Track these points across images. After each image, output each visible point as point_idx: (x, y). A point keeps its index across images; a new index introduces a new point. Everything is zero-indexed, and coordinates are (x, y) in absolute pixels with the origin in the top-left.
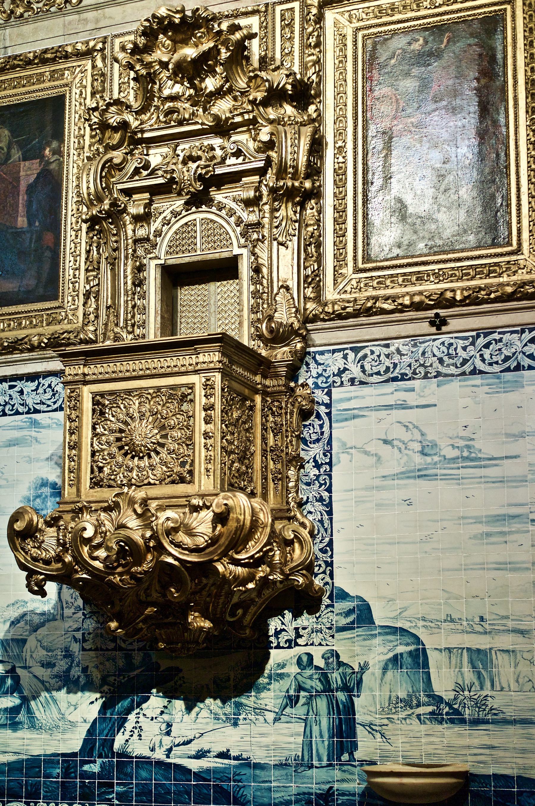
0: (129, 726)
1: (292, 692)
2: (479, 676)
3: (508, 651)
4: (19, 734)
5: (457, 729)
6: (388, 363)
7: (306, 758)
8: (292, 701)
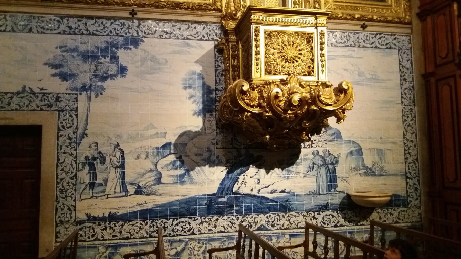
0: (240, 181)
1: (311, 166)
2: (381, 159)
3: (390, 150)
4: (185, 186)
5: (374, 178)
6: (345, 39)
7: (317, 191)
8: (311, 169)
